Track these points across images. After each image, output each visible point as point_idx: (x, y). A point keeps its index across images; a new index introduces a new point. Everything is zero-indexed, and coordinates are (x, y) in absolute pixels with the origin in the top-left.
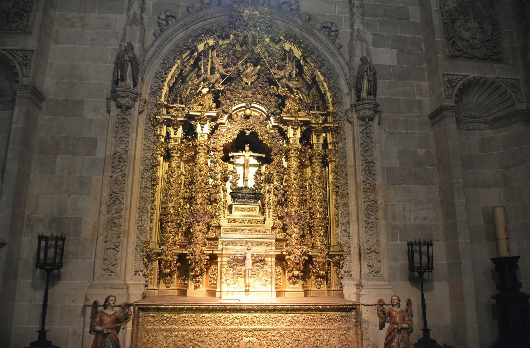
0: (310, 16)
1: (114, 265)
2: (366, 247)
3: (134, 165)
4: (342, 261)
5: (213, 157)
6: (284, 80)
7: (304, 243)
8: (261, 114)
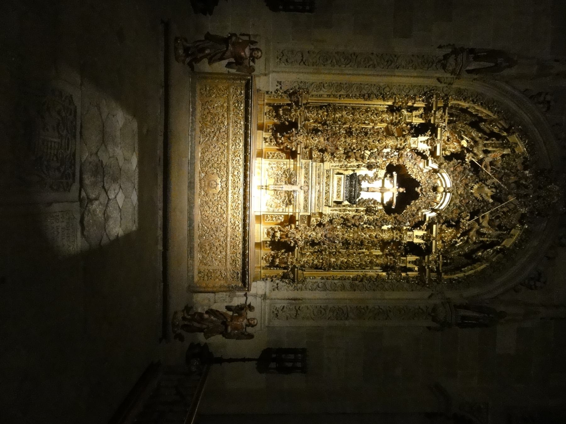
1: (287, 61)
2: (302, 306)
4: (288, 282)
5: (392, 155)
6: (477, 226)
8: (437, 204)
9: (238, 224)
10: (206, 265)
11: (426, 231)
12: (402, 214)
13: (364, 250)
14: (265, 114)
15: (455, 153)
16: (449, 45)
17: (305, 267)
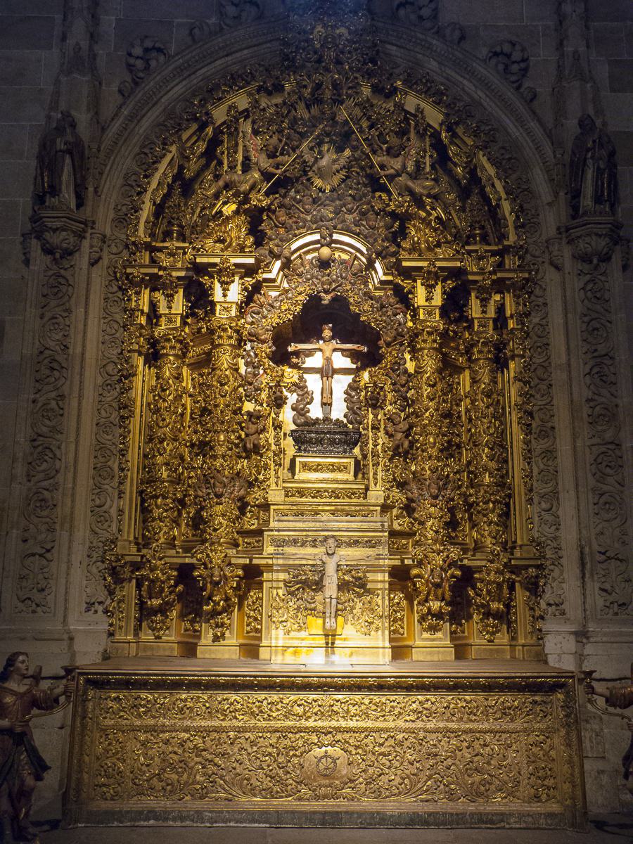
0: (461, 29)
1: (43, 590)
2: (596, 547)
3: (81, 375)
4: (543, 580)
5: (252, 354)
6: (402, 179)
7: (456, 541)
8: (356, 257)
9: (417, 702)
11: (415, 281)
12: (381, 330)
13: (462, 409)
14: (158, 640)
15: (249, 226)
17: (506, 542)
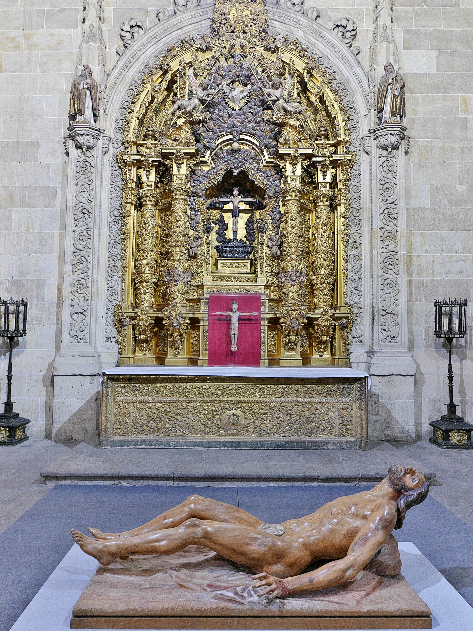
5: (194, 203)
10: (334, 427)
16: (64, 143)
